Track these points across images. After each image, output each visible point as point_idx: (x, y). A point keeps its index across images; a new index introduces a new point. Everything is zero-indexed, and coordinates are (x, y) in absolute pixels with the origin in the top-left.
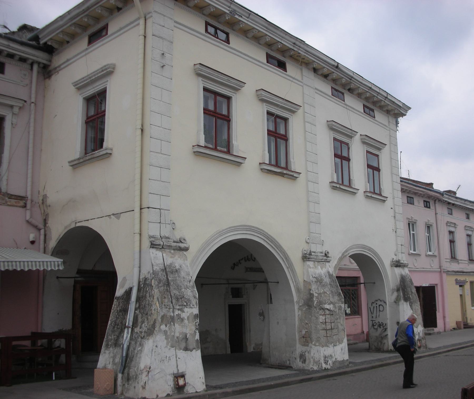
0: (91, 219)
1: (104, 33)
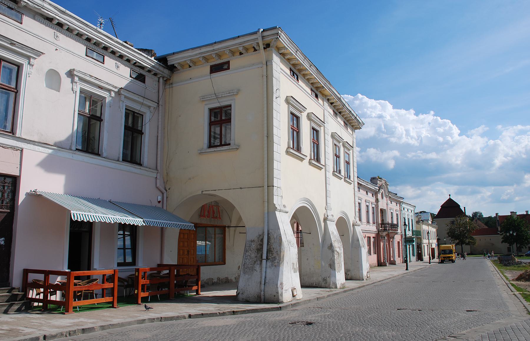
0: (218, 190)
1: (226, 67)
